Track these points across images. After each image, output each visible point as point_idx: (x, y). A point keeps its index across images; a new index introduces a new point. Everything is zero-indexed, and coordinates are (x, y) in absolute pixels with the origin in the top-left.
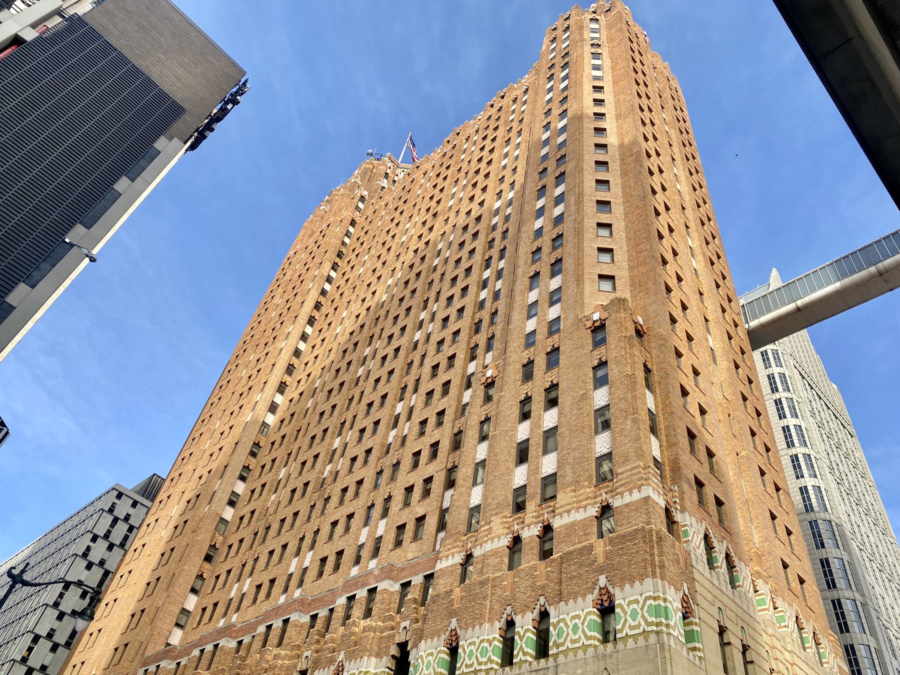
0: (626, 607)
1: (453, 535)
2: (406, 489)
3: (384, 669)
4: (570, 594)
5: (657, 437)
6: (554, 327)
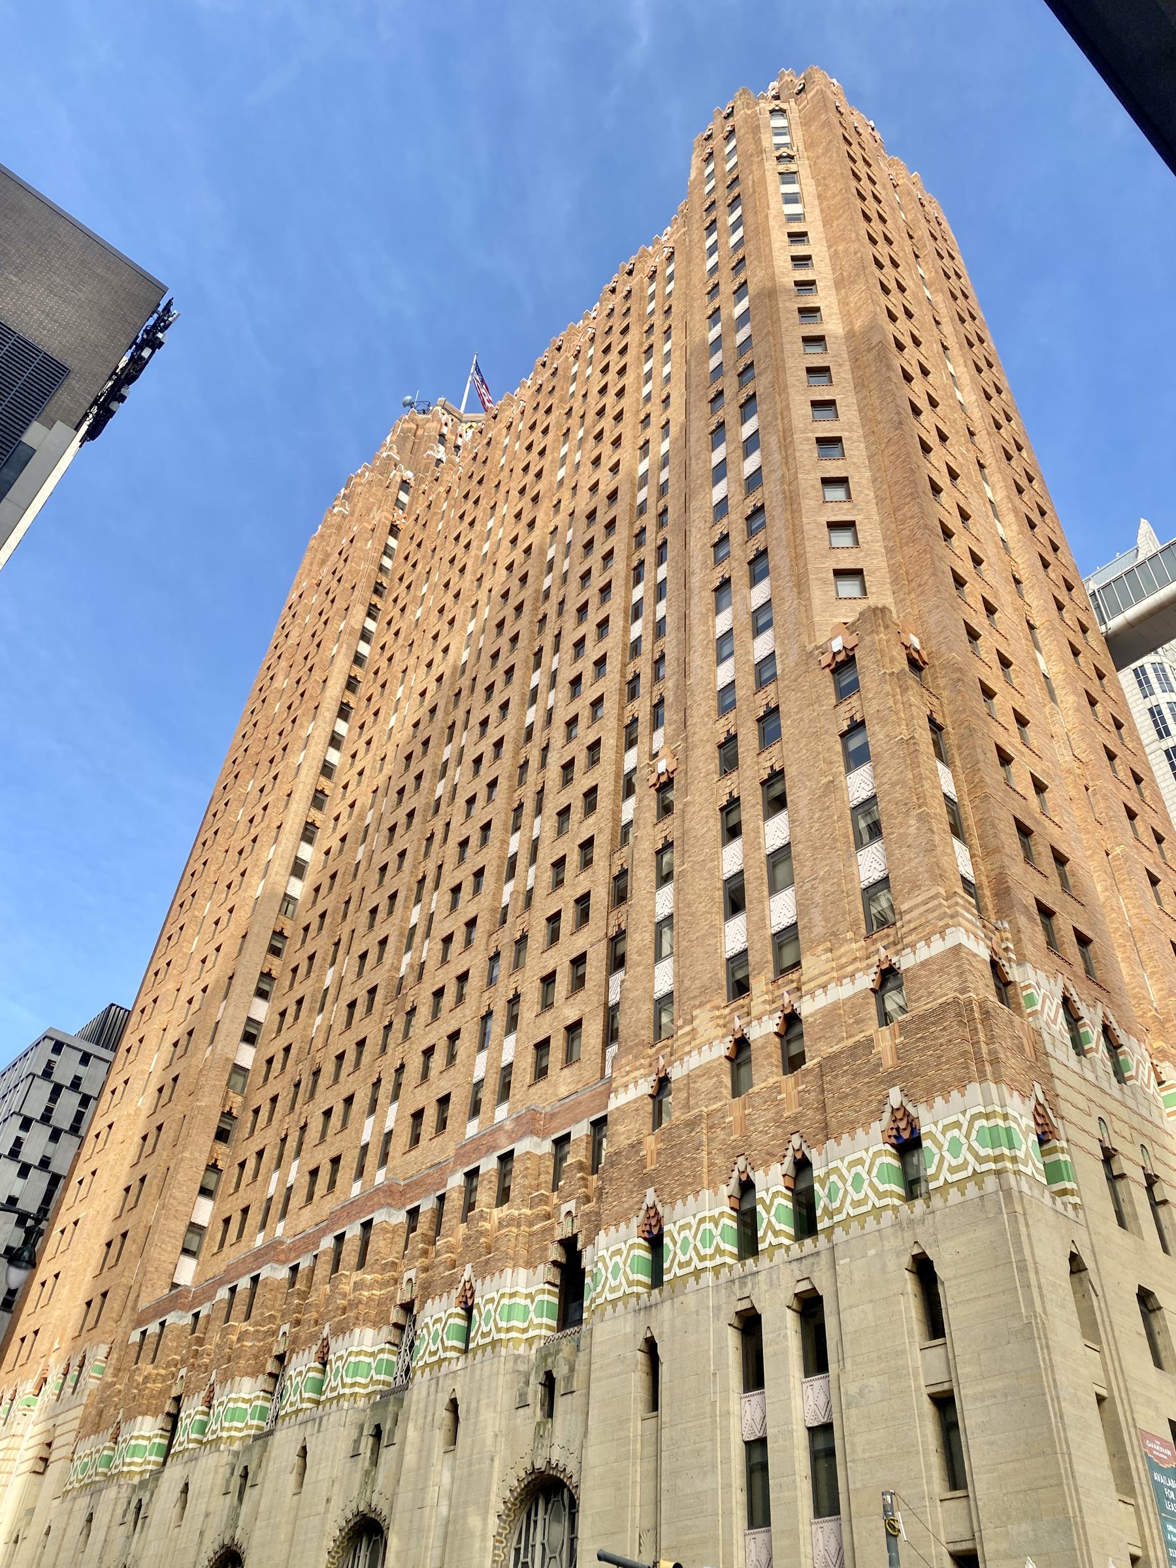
0: (939, 1136)
1: (632, 1048)
2: (543, 980)
3: (541, 1286)
4: (841, 1125)
5: (964, 842)
6: (765, 671)
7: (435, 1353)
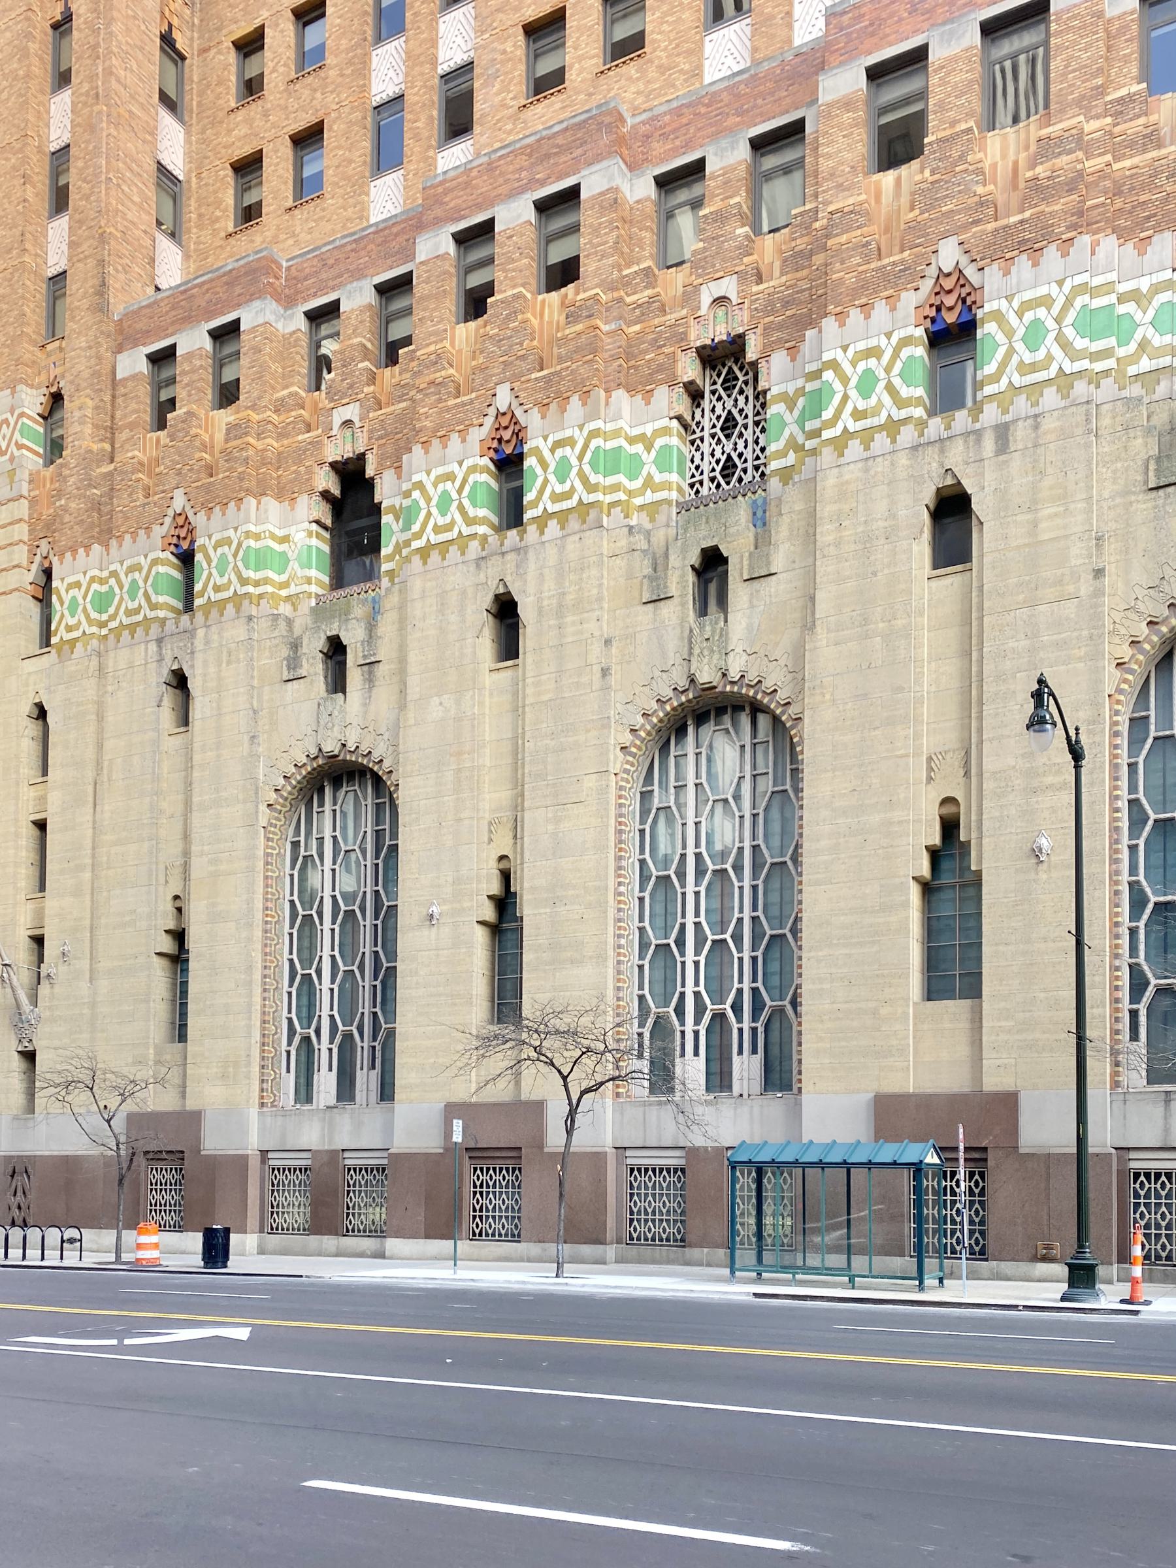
7: (137, 611)
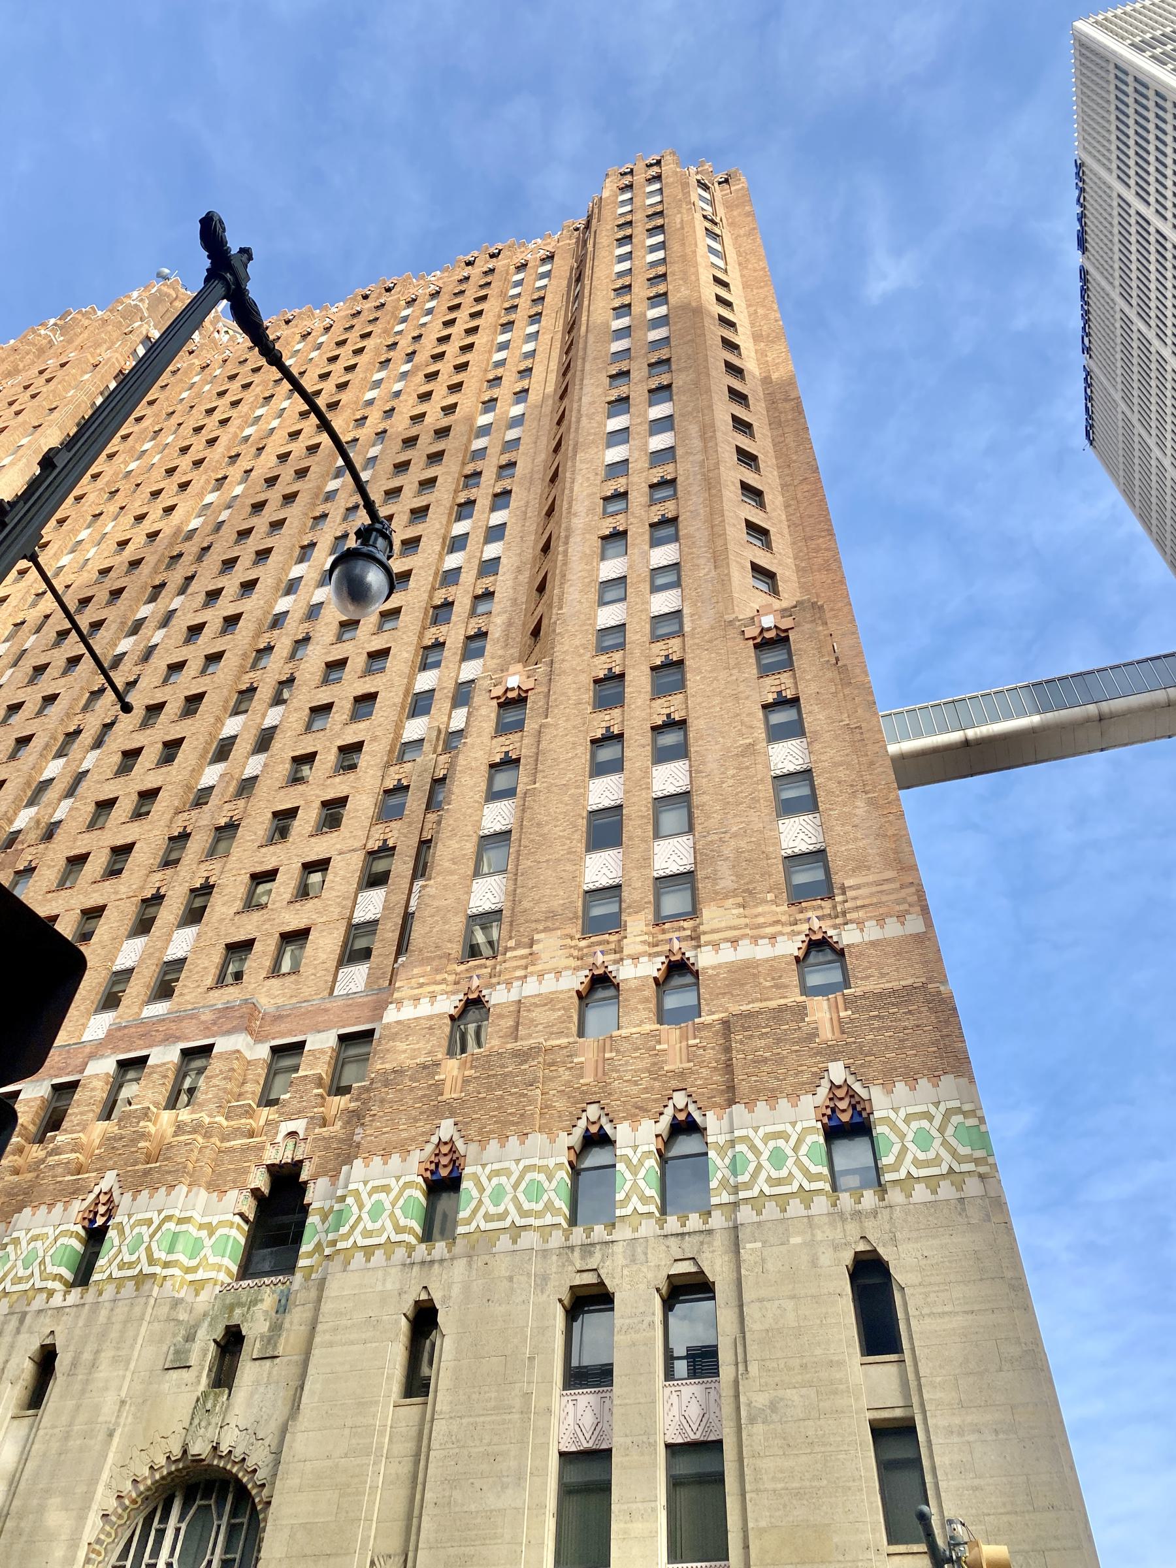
1: (433, 959)
3: (230, 1217)
